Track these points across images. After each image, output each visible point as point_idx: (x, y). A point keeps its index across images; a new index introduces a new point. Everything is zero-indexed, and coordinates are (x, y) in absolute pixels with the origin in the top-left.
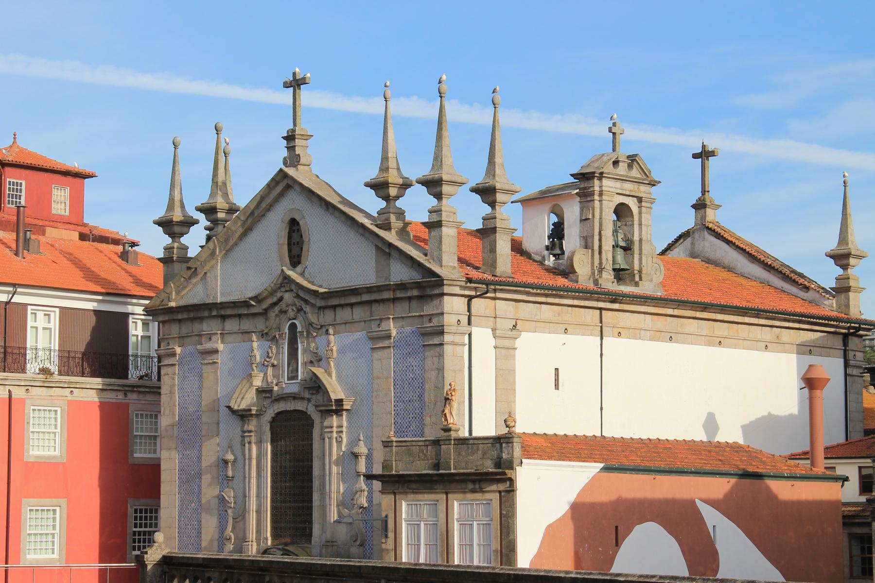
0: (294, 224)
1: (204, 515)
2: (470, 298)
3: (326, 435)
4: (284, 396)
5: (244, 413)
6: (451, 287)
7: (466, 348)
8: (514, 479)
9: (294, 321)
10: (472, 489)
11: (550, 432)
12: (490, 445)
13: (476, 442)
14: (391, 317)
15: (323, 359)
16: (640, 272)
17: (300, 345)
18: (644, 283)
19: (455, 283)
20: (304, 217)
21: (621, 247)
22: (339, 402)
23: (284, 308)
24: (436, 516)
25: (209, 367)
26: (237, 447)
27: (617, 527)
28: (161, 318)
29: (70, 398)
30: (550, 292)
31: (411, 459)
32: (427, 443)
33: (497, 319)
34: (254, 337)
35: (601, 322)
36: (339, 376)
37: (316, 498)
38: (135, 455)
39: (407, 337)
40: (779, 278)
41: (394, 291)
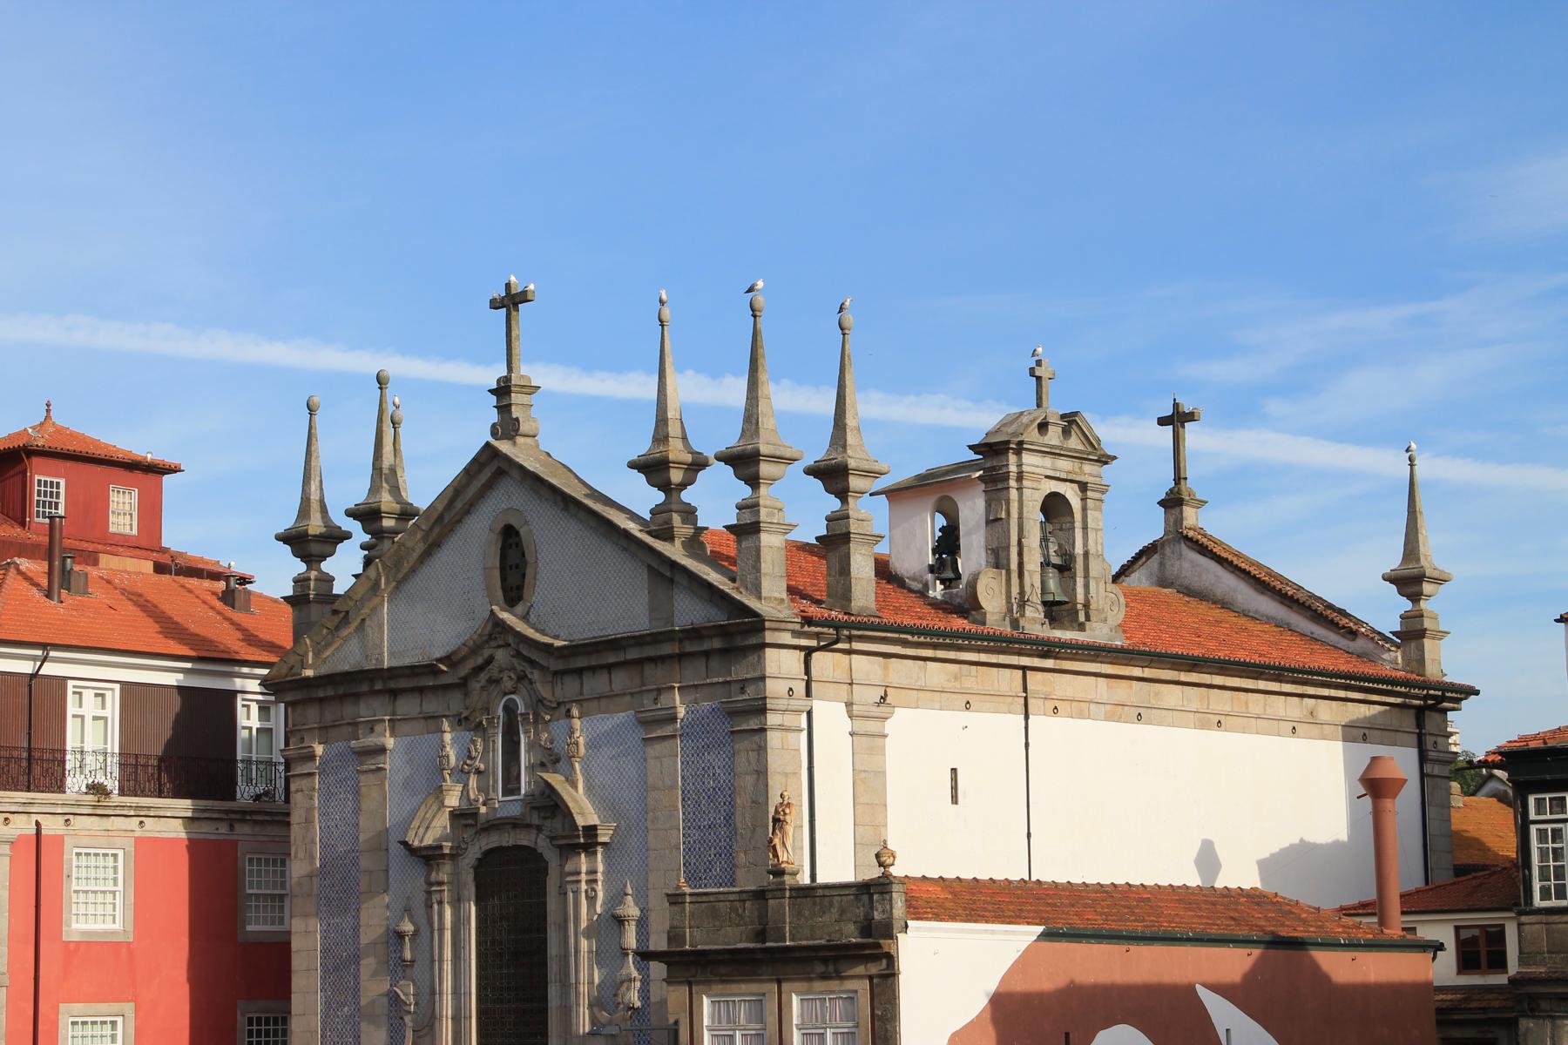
0: (510, 537)
1: (364, 1026)
2: (809, 652)
3: (569, 887)
4: (495, 822)
5: (430, 853)
6: (777, 634)
7: (804, 735)
8: (895, 955)
9: (513, 696)
10: (822, 973)
11: (950, 874)
12: (852, 897)
13: (827, 892)
14: (677, 685)
15: (563, 759)
16: (1087, 606)
17: (522, 736)
18: (1095, 625)
19: (783, 626)
20: (526, 523)
21: (1055, 566)
22: (591, 830)
23: (496, 675)
24: (761, 1020)
25: (371, 776)
26: (420, 910)
27: (1067, 1034)
28: (290, 697)
29: (139, 833)
30: (941, 641)
31: (717, 923)
32: (744, 896)
33: (854, 686)
34: (446, 725)
35: (1025, 690)
36: (589, 789)
37: (554, 993)
38: (249, 928)
39: (703, 719)
40: (1306, 617)
41: (681, 641)
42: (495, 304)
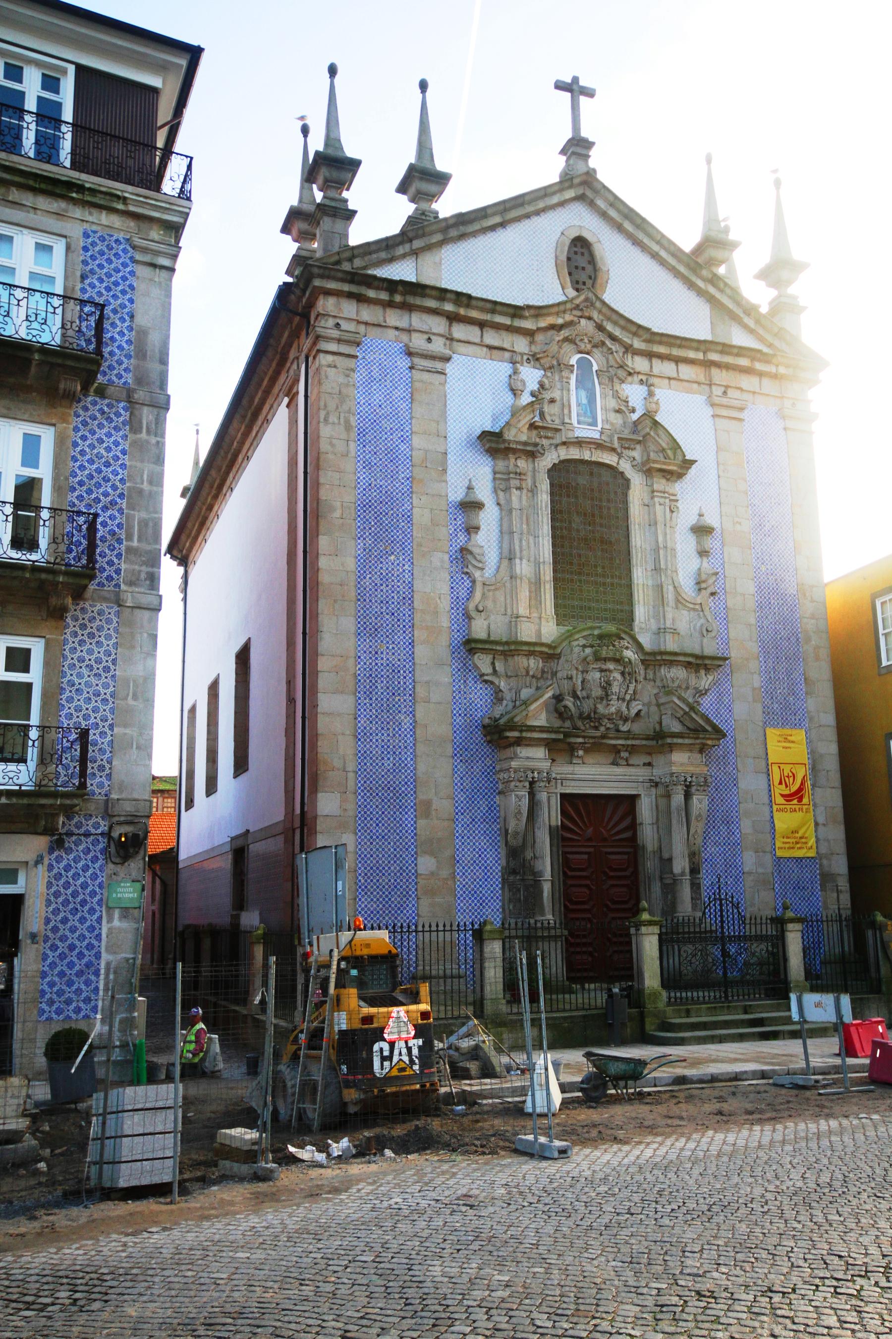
42: (560, 86)
